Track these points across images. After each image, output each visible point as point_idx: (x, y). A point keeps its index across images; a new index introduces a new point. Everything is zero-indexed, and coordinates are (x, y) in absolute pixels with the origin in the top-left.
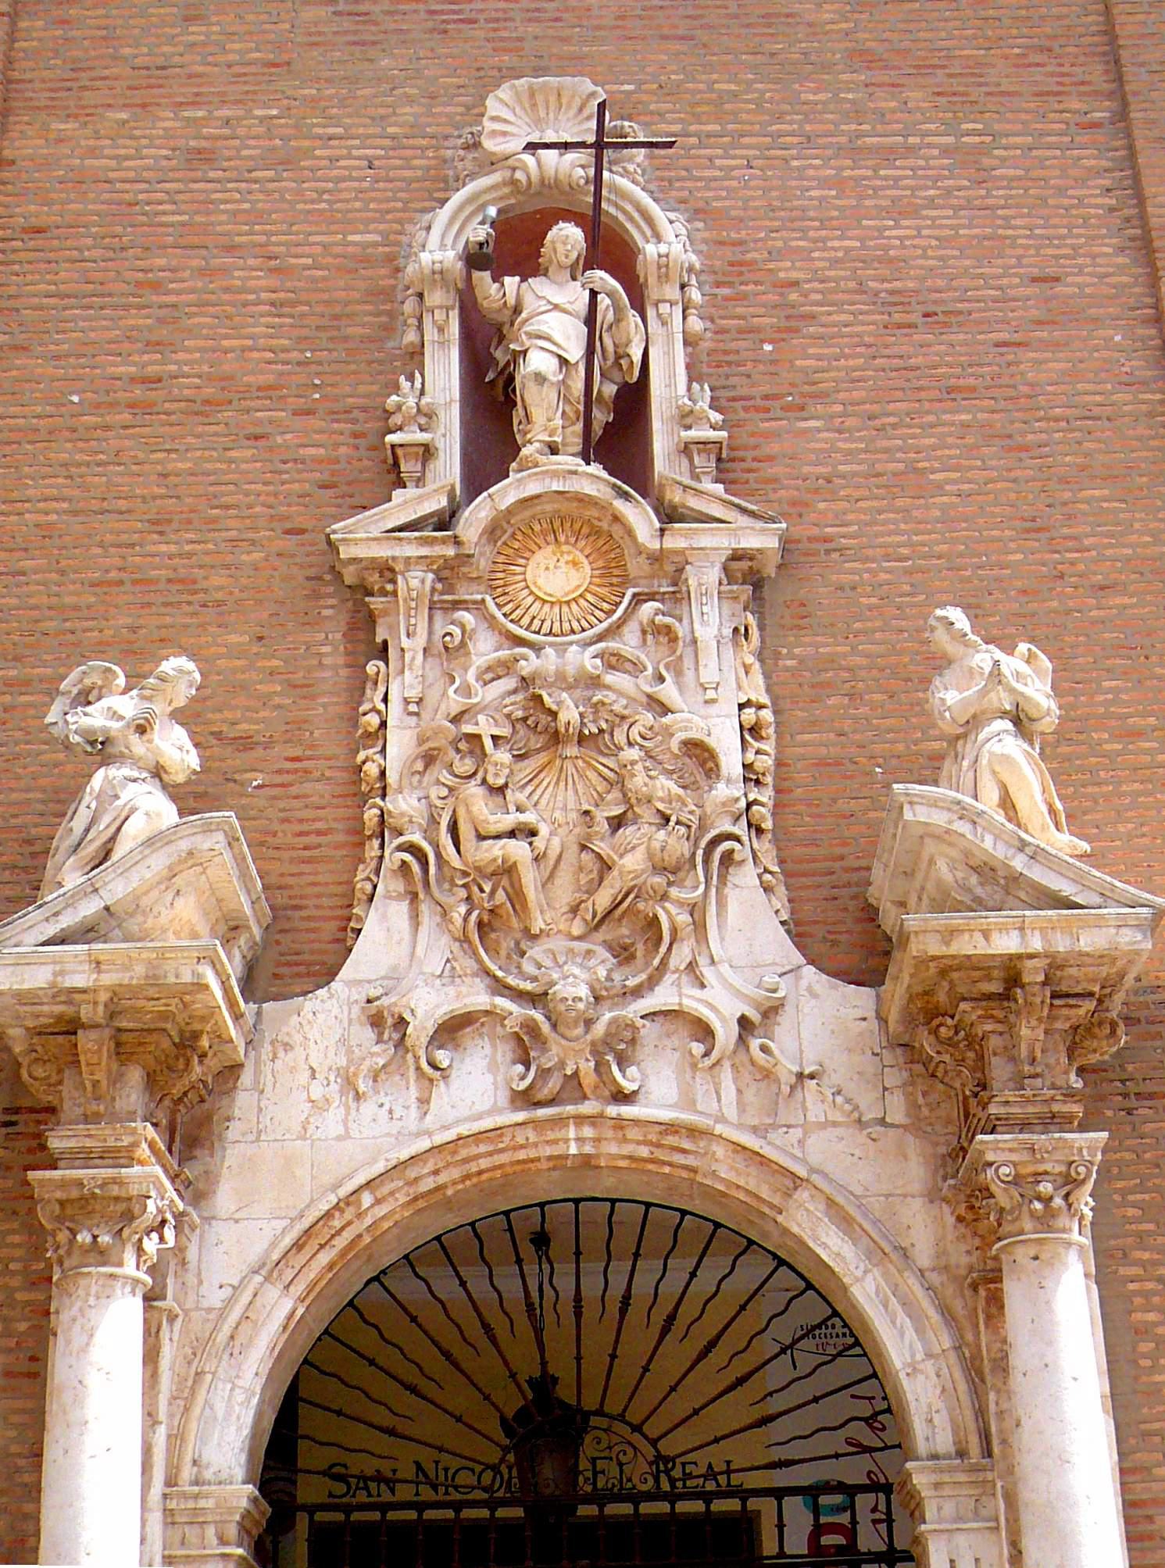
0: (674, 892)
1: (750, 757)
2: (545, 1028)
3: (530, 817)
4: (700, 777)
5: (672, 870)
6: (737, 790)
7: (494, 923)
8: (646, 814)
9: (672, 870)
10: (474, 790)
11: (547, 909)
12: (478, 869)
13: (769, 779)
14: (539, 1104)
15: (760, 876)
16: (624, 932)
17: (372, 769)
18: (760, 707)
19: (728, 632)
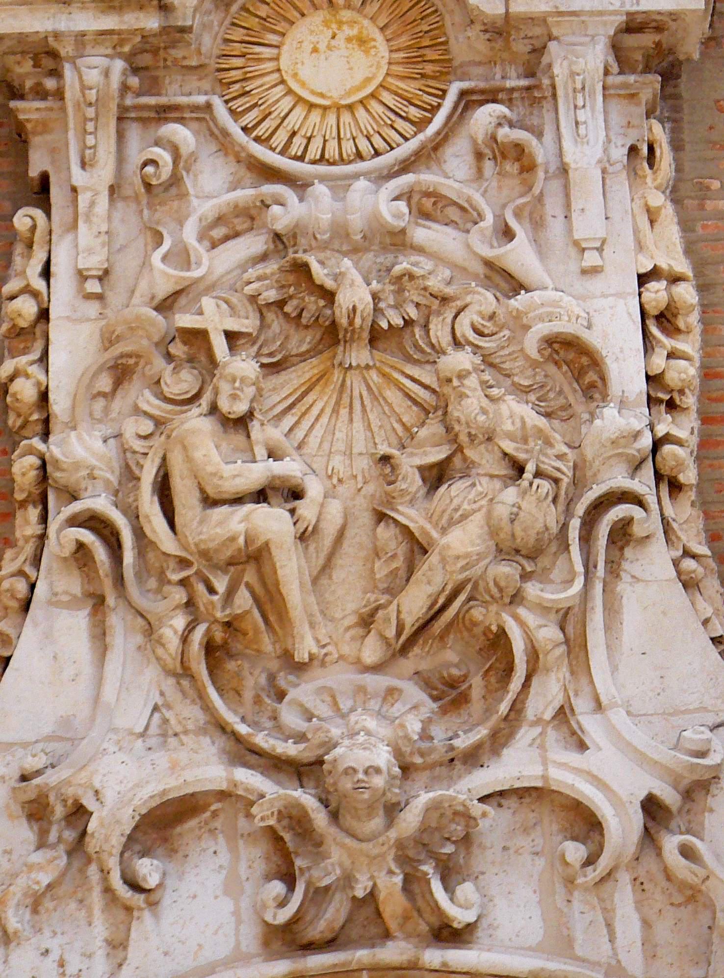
0: (532, 590)
1: (659, 362)
2: (320, 818)
3: (290, 468)
4: (575, 398)
5: (529, 554)
6: (636, 419)
7: (232, 643)
8: (486, 460)
9: (529, 554)
10: (196, 424)
11: (322, 616)
12: (205, 554)
13: (690, 401)
14: (310, 947)
15: (676, 563)
16: (450, 657)
17: (25, 390)
18: (675, 279)
19: (620, 153)
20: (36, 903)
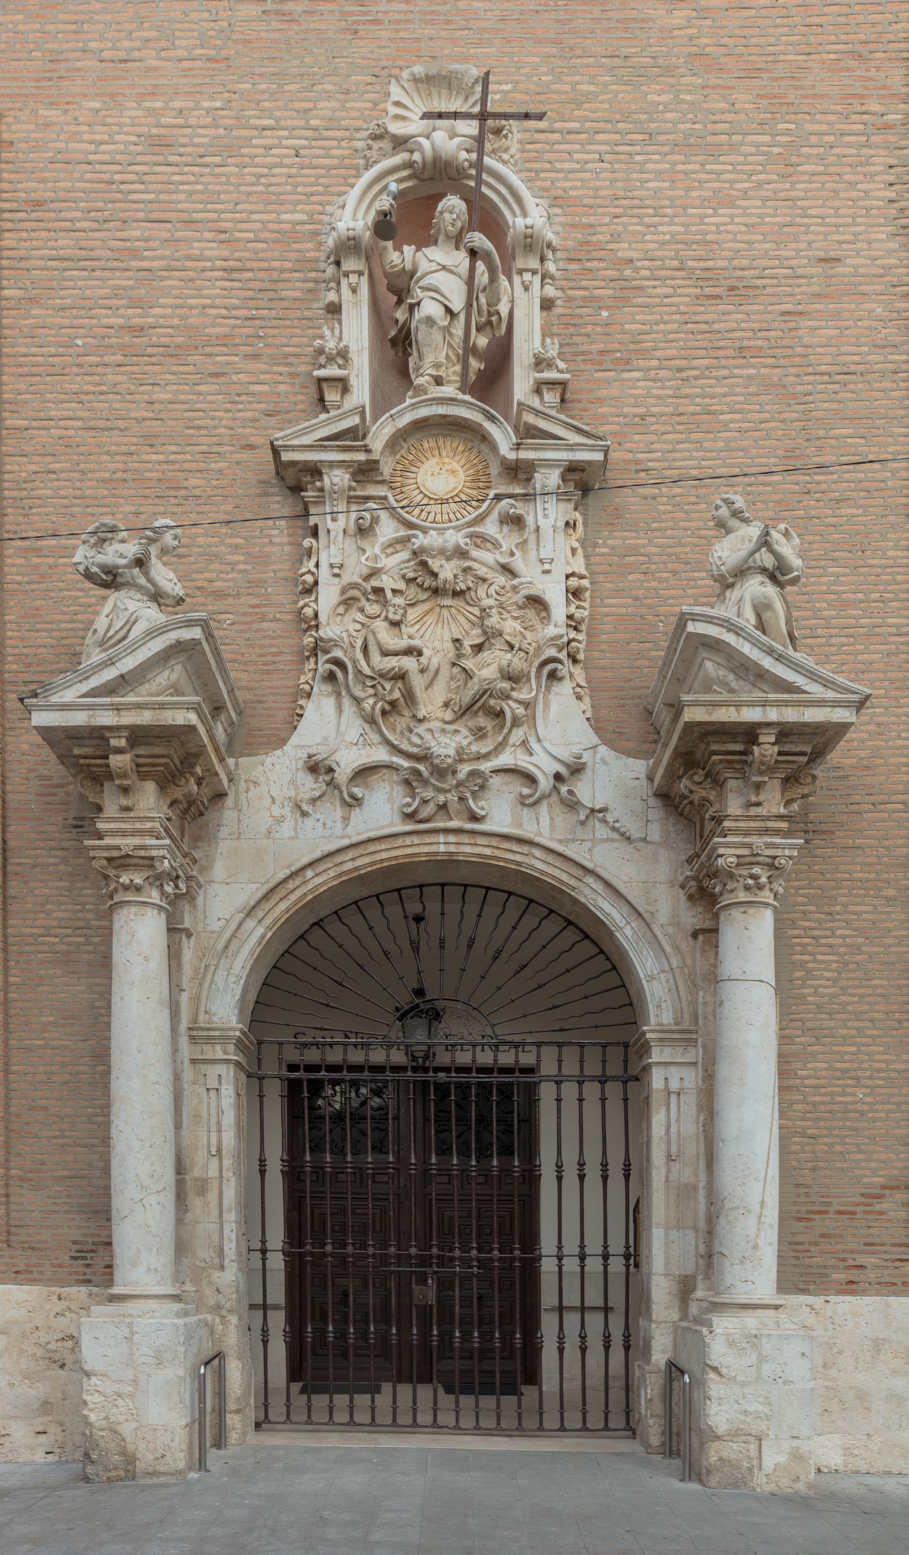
0: (514, 694)
3: (416, 642)
7: (394, 701)
9: (513, 678)
10: (380, 625)
14: (421, 821)
20: (314, 801)
